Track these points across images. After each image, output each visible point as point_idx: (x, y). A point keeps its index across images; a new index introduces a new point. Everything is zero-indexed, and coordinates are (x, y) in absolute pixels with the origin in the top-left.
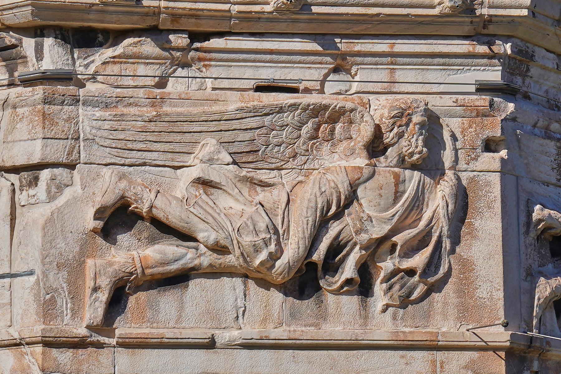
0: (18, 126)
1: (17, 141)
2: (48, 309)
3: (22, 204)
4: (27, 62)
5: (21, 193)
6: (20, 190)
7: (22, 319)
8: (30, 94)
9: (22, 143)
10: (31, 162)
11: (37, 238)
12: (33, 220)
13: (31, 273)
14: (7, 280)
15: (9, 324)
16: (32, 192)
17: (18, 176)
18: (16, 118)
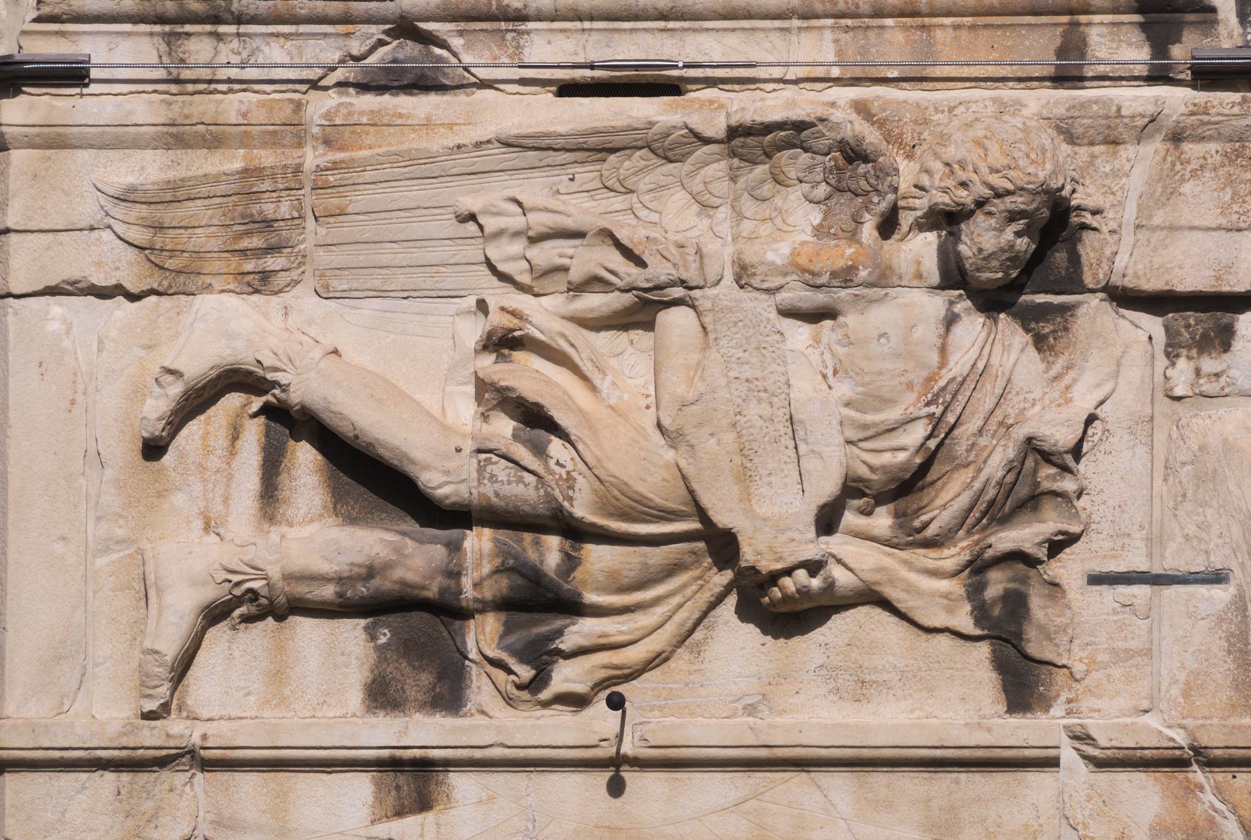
0: (1187, 188)
1: (1180, 228)
3: (1178, 392)
4: (1215, 22)
5: (1173, 364)
6: (1168, 355)
7: (1186, 694)
8: (1236, 110)
9: (1198, 235)
10: (1226, 289)
12: (1225, 441)
13: (1217, 578)
14: (1140, 592)
15: (1145, 704)
16: (1209, 364)
17: (1159, 320)
18: (1178, 167)
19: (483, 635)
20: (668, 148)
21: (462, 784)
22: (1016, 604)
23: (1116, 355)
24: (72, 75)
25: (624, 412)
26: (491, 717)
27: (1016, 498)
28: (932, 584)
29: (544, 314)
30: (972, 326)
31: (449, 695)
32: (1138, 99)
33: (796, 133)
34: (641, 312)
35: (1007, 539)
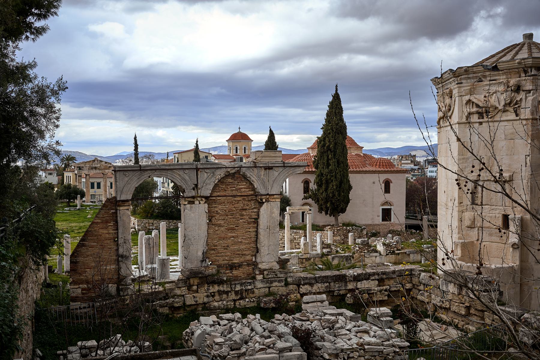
2: (532, 114)
11: (531, 102)
19: (484, 115)
20: (495, 84)
21: (484, 124)
22: (516, 110)
23: (522, 95)
24: (462, 83)
25: (493, 101)
26: (486, 119)
27: (516, 104)
28: (511, 109)
29: (487, 95)
30: (513, 94)
31: (483, 118)
32: (524, 78)
33: (501, 83)
34: (492, 95)
35: (516, 106)
